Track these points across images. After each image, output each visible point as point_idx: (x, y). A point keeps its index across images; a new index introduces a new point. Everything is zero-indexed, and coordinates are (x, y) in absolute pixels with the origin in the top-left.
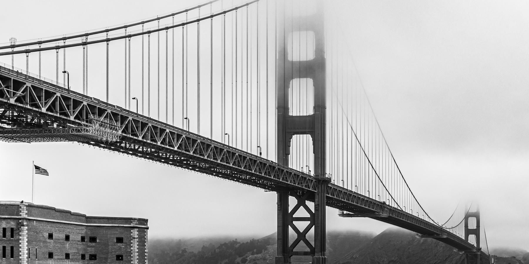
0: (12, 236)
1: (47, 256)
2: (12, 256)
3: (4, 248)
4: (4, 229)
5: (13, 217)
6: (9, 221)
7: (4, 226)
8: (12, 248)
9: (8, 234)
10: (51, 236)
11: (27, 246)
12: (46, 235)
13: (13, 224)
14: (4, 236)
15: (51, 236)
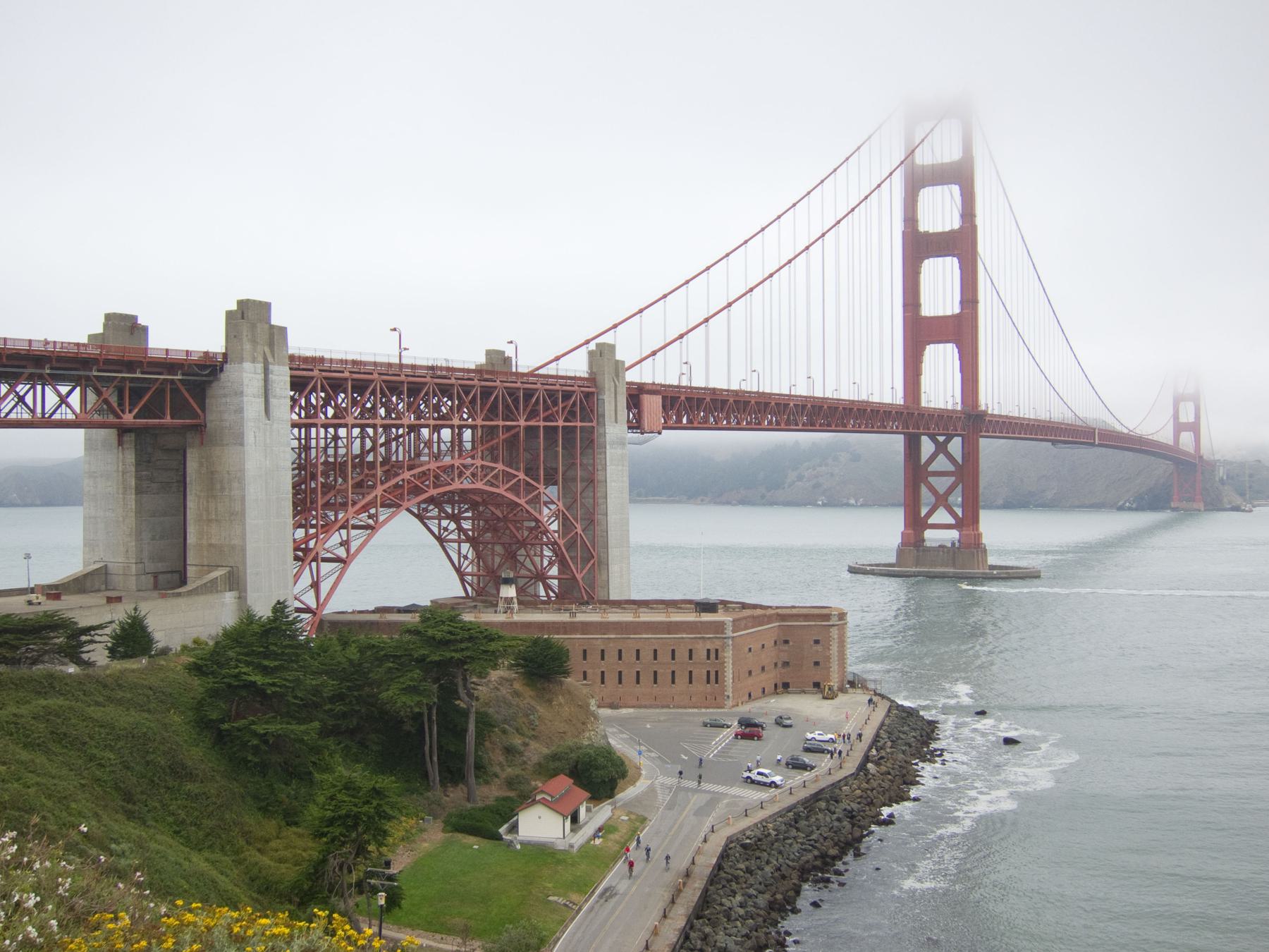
0: (717, 658)
1: (747, 675)
2: (717, 682)
3: (708, 672)
4: (708, 651)
5: (718, 636)
6: (714, 640)
7: (709, 647)
8: (717, 672)
9: (713, 655)
10: (750, 650)
11: (732, 668)
12: (747, 649)
13: (717, 644)
14: (708, 658)
15: (750, 650)
